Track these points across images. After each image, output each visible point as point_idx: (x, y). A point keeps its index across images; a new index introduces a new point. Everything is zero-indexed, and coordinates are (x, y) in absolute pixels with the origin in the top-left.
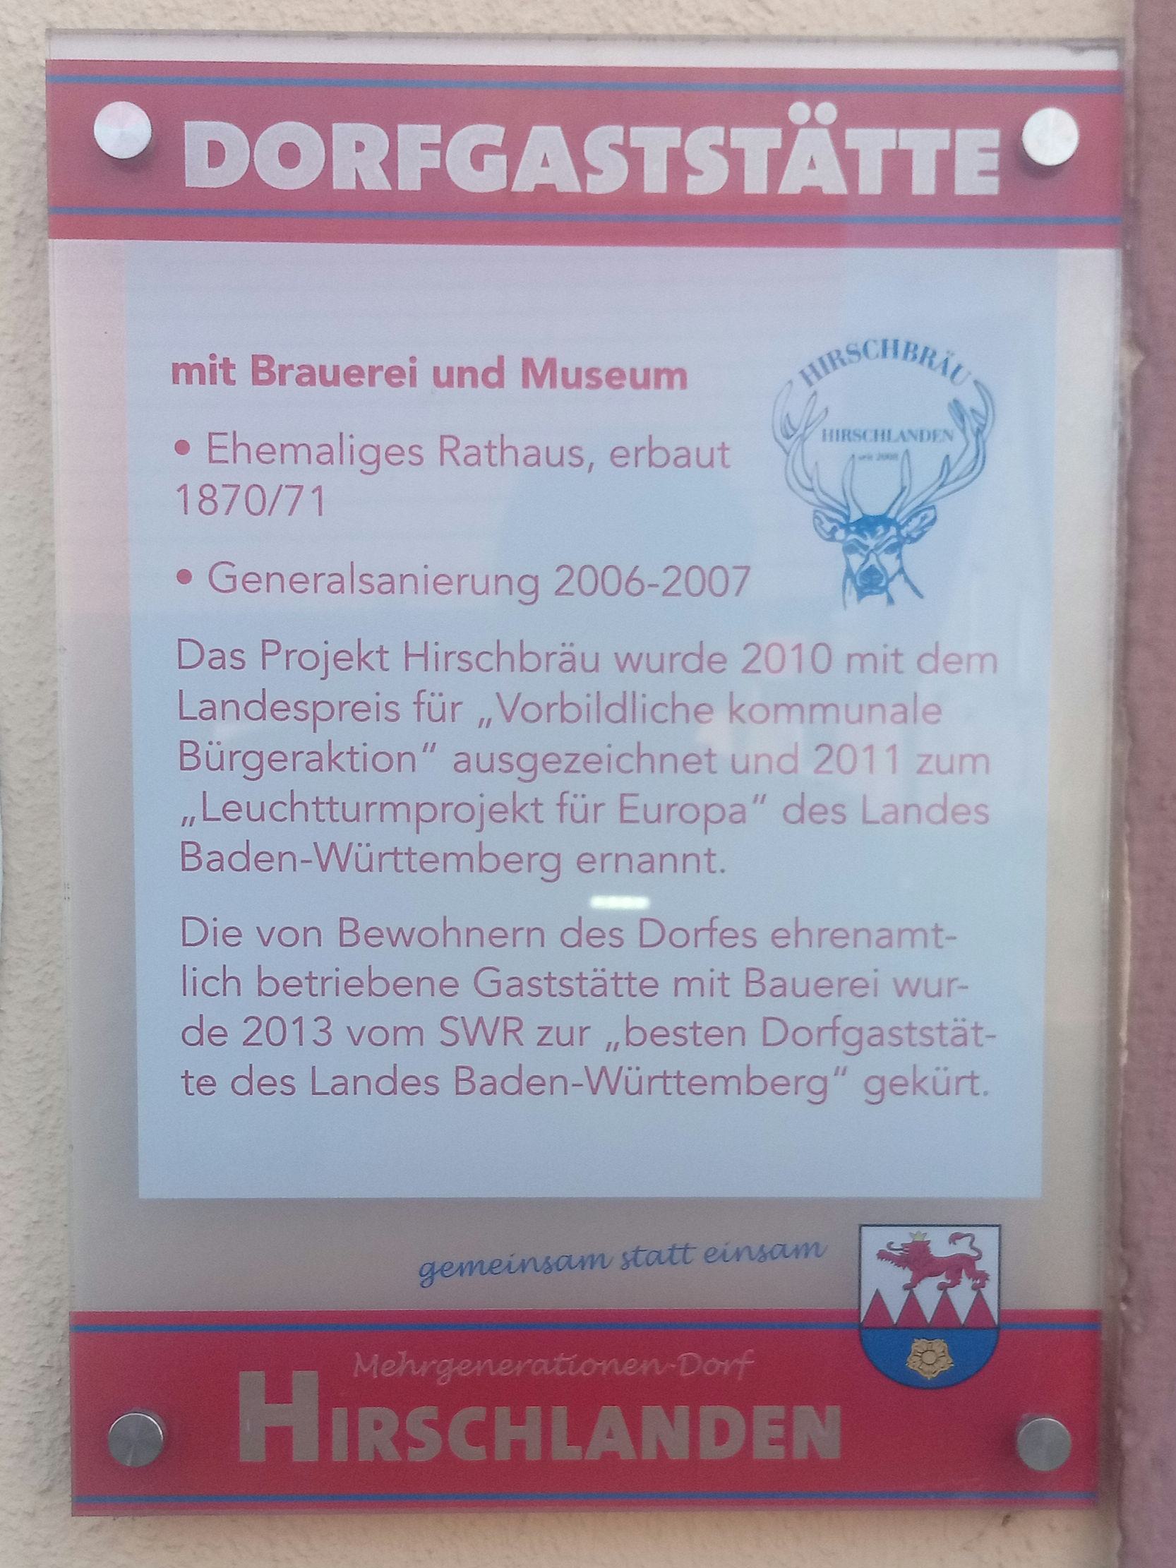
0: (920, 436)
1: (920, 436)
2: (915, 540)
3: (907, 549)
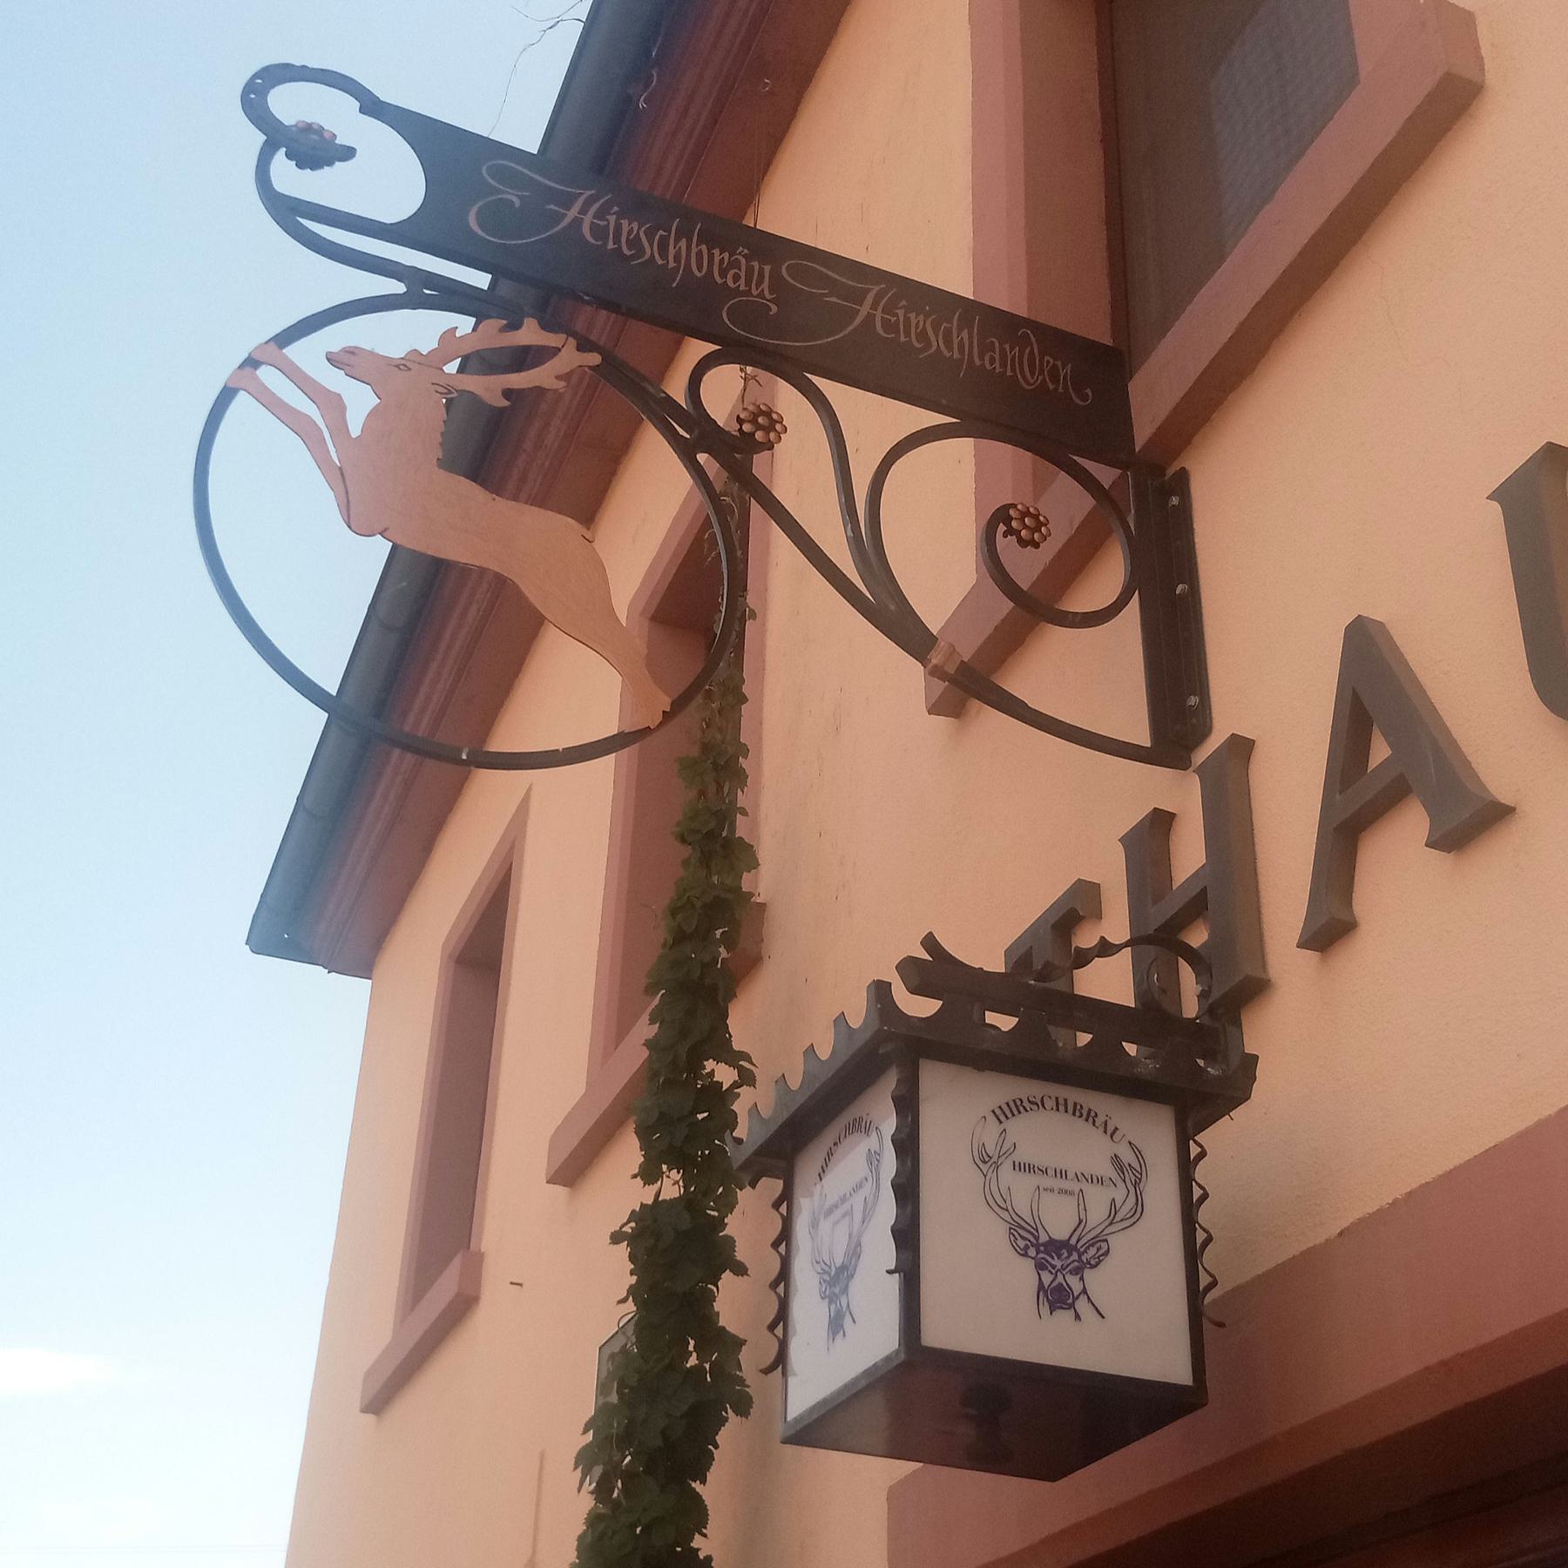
0: (1091, 1180)
1: (1091, 1180)
2: (1093, 1267)
3: (1088, 1273)
